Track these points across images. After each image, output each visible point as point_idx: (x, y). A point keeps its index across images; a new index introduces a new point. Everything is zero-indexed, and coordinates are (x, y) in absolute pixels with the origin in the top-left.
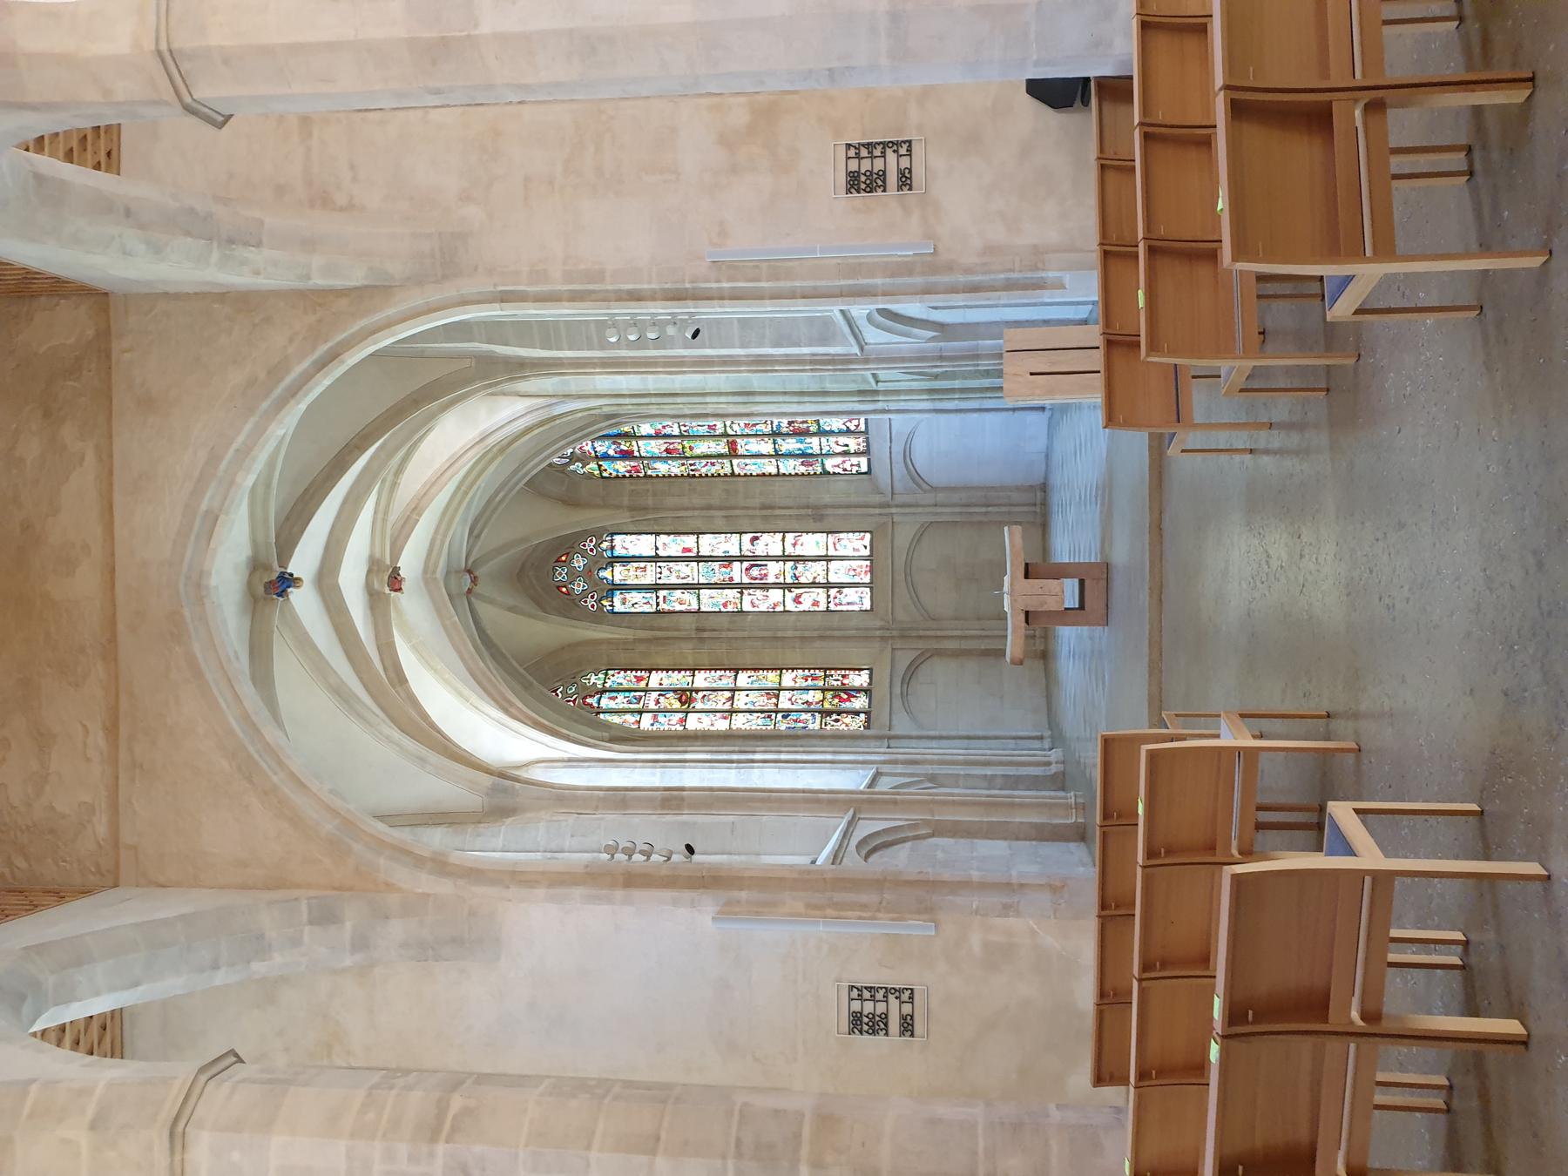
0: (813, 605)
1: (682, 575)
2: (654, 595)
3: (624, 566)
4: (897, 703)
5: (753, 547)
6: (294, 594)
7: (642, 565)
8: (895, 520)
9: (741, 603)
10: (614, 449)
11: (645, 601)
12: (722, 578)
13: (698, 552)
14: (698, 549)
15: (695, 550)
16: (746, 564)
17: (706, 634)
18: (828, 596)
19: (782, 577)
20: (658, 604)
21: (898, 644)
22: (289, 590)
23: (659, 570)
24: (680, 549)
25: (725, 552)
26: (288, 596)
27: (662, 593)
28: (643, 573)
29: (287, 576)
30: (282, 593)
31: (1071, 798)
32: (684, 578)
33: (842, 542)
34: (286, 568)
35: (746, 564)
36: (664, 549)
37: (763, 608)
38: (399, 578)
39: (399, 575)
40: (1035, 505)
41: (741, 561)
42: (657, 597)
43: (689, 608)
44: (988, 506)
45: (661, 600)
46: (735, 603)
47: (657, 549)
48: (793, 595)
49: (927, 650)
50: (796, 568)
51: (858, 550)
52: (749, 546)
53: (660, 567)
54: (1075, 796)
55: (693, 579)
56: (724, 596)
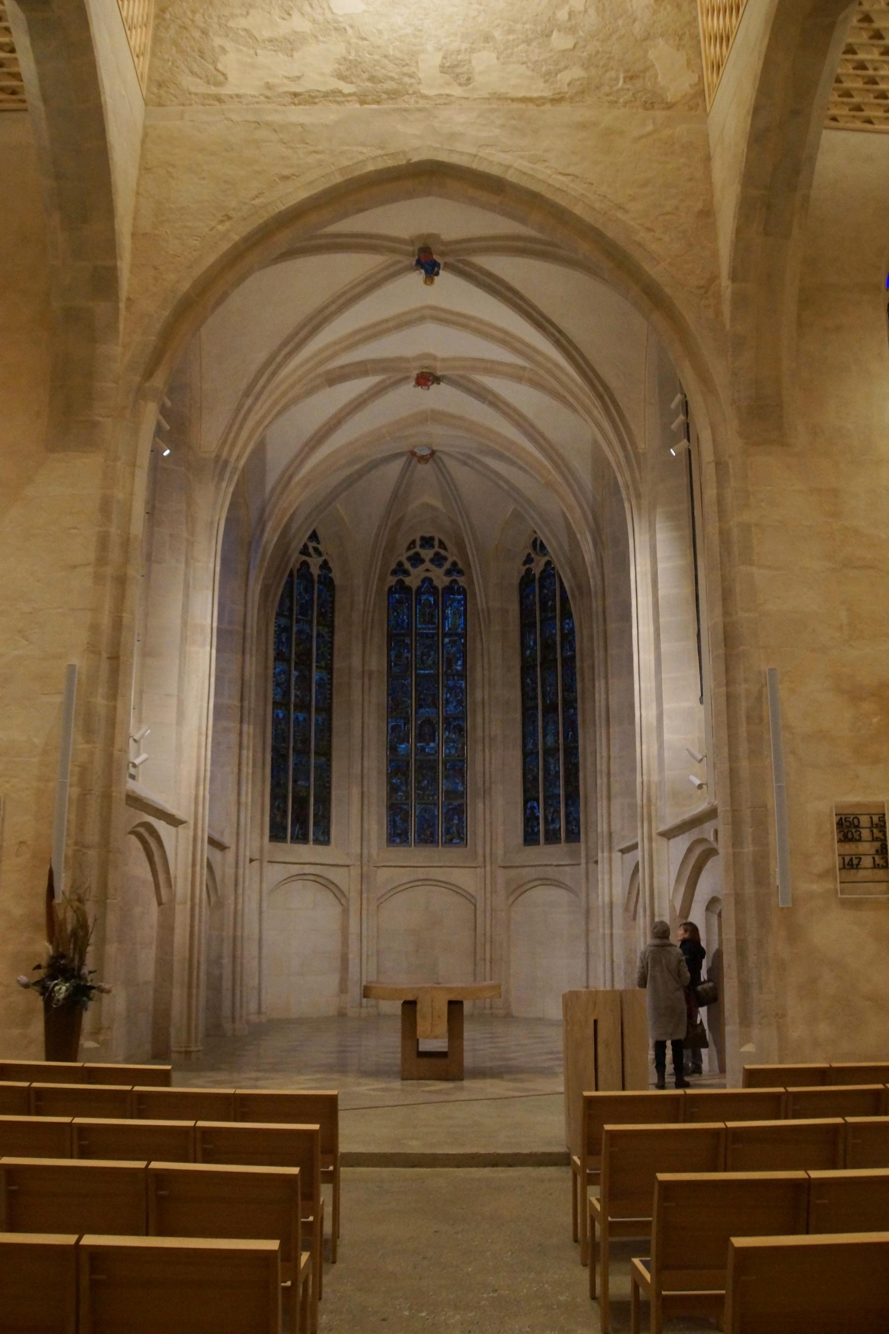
1: (425, 658)
4: (295, 869)
6: (418, 276)
8: (478, 869)
10: (547, 594)
17: (366, 680)
21: (355, 872)
22: (423, 271)
26: (417, 270)
29: (436, 269)
30: (420, 264)
31: (196, 1046)
34: (443, 270)
38: (430, 383)
39: (433, 383)
40: (491, 1008)
44: (491, 962)
49: (348, 900)
54: (198, 1051)
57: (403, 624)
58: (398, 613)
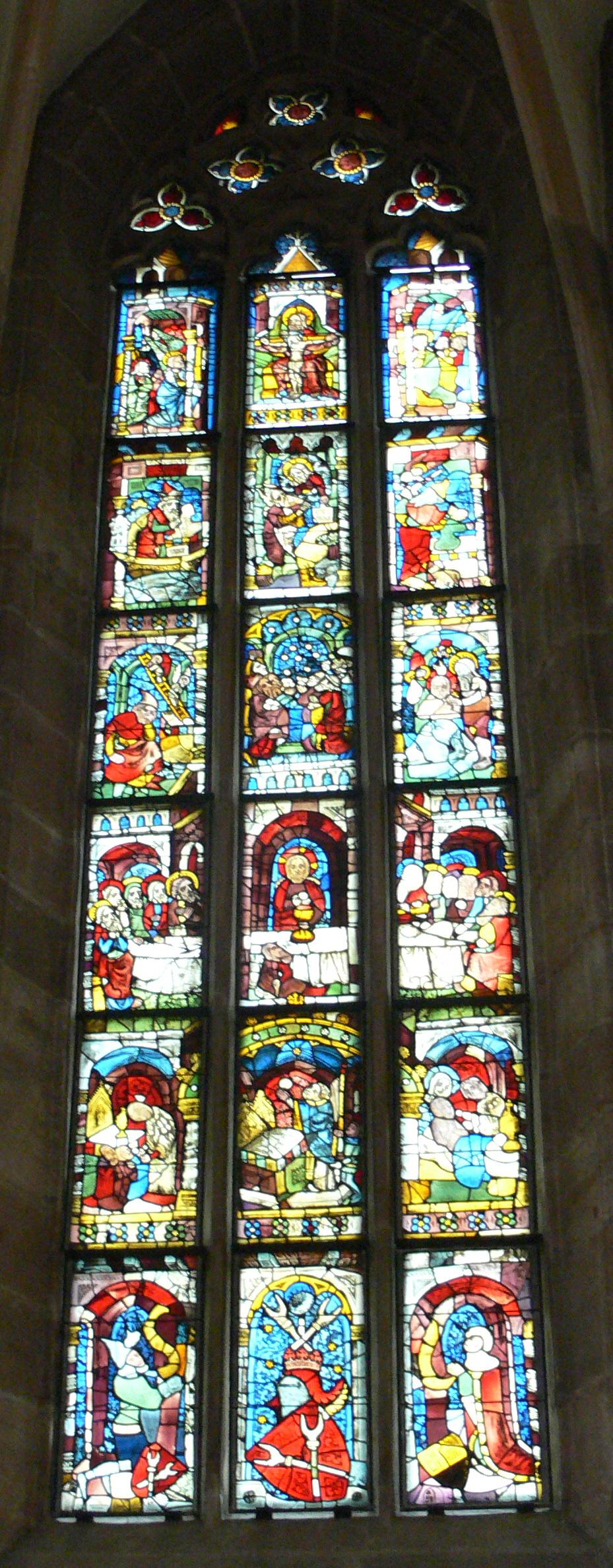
0: (106, 1169)
1: (283, 535)
2: (188, 430)
3: (331, 314)
5: (439, 839)
7: (338, 379)
9: (132, 802)
11: (164, 394)
12: (271, 705)
13: (410, 598)
14: (423, 596)
15: (416, 583)
16: (338, 814)
18: (153, 1258)
19: (269, 1000)
20: (145, 446)
23: (310, 440)
24: (422, 519)
25: (409, 712)
27: (198, 466)
28: (296, 381)
32: (270, 542)
33: (480, 1338)
35: (338, 814)
36: (418, 458)
37: (101, 910)
41: (351, 796)
42: (178, 444)
43: (119, 570)
45: (170, 459)
46: (130, 772)
47: (420, 430)
48: (171, 1066)
50: (323, 1075)
51: (436, 1430)
52: (447, 824)
53: (325, 445)
55: (261, 583)
56: (173, 720)
57: (177, 402)
58: (154, 366)
